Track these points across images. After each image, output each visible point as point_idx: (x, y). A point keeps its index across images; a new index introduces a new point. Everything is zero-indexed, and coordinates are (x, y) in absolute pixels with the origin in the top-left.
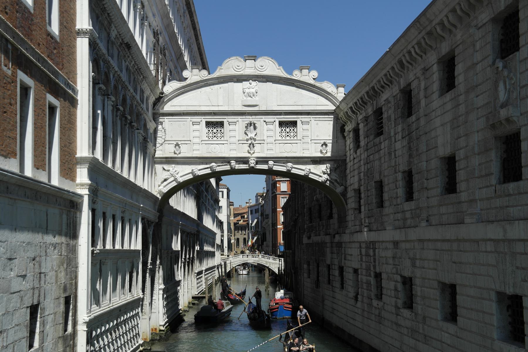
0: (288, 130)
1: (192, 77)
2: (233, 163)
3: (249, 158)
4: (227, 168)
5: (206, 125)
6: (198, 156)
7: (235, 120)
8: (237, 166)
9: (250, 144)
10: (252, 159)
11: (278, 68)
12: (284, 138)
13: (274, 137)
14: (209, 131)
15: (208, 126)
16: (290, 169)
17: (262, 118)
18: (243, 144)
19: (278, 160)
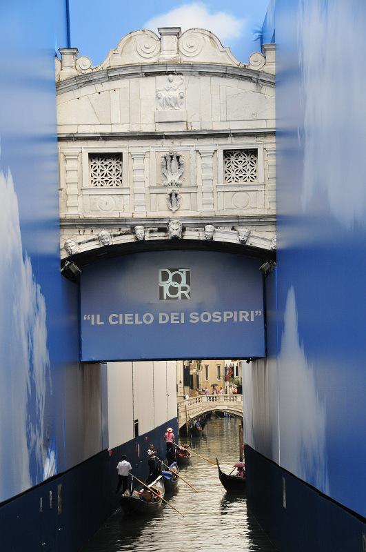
0: (240, 167)
1: (61, 70)
2: (140, 231)
4: (129, 239)
6: (76, 217)
7: (144, 150)
8: (148, 234)
9: (171, 195)
10: (175, 221)
11: (221, 49)
13: (215, 181)
14: (96, 171)
15: (94, 161)
16: (245, 239)
17: (192, 146)
19: (219, 221)
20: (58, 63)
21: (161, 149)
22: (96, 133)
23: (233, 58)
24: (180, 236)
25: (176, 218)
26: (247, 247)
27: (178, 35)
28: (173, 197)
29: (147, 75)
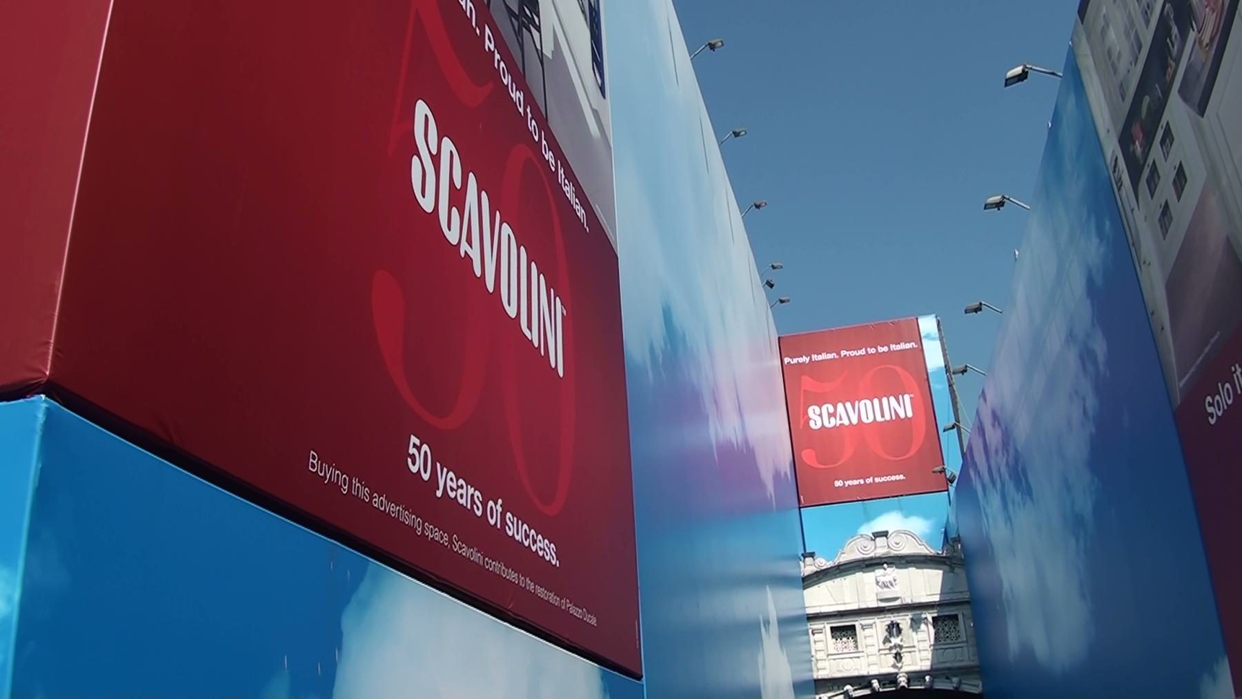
0: (946, 629)
2: (875, 683)
3: (897, 674)
4: (867, 692)
5: (832, 632)
6: (826, 677)
9: (896, 654)
12: (942, 641)
15: (835, 632)
18: (885, 654)
20: (801, 563)
21: (885, 619)
22: (835, 612)
23: (929, 548)
24: (906, 686)
25: (902, 672)
26: (960, 692)
27: (886, 536)
28: (898, 657)
29: (868, 566)
